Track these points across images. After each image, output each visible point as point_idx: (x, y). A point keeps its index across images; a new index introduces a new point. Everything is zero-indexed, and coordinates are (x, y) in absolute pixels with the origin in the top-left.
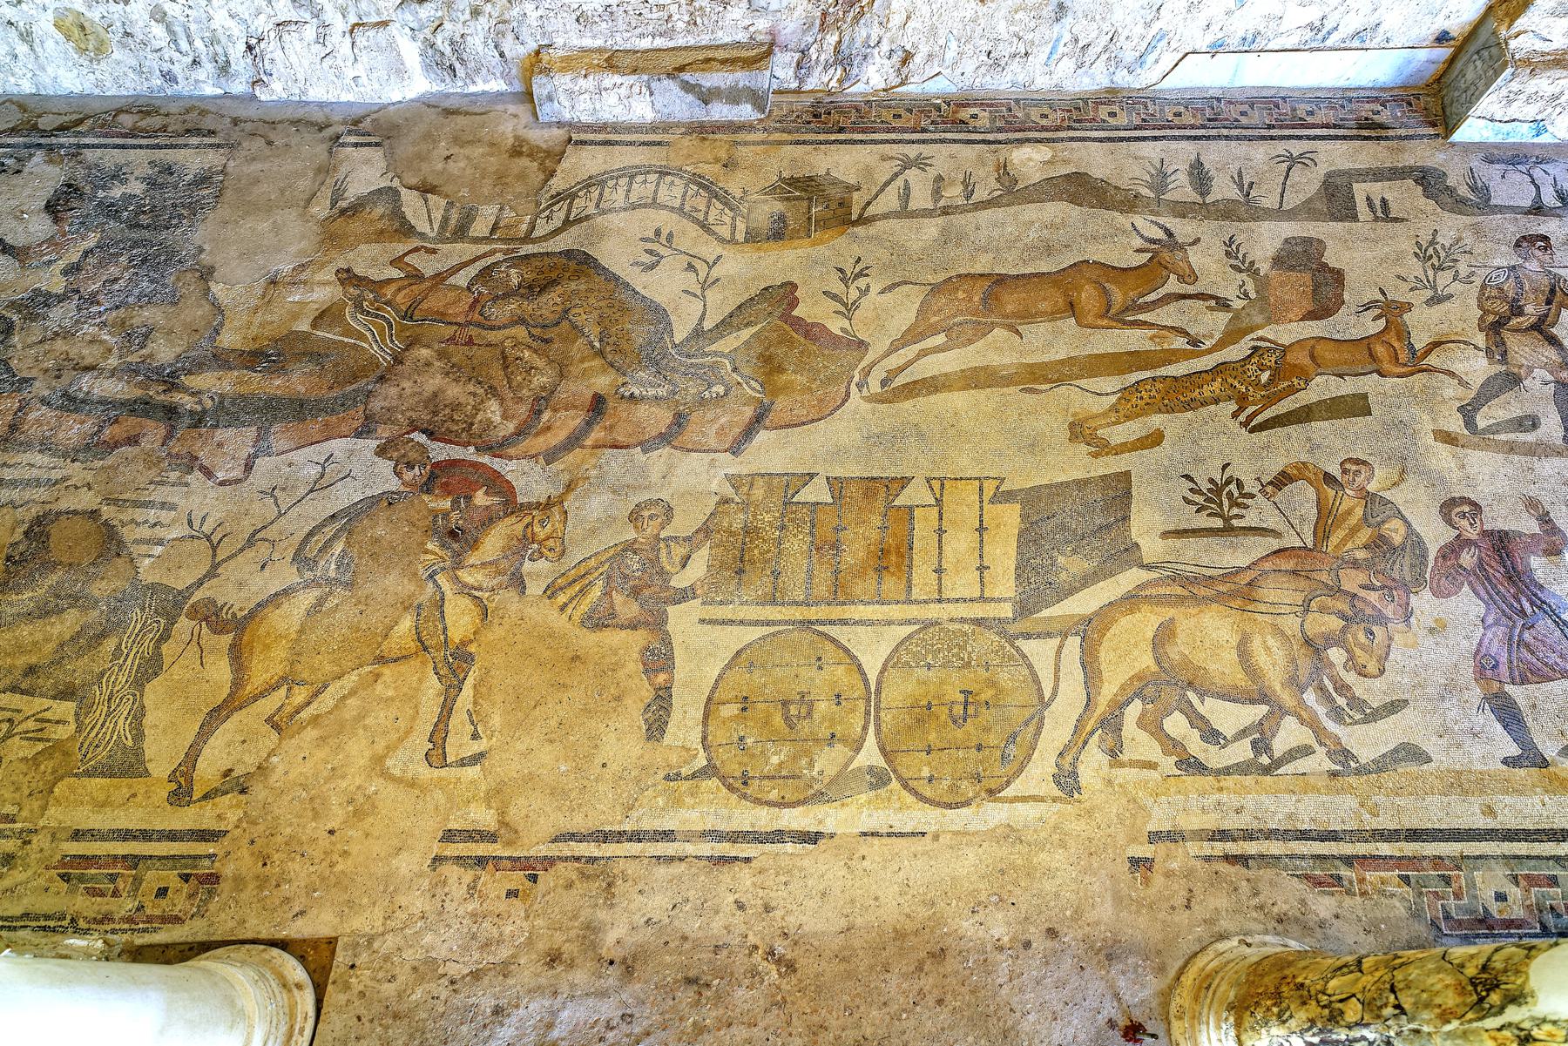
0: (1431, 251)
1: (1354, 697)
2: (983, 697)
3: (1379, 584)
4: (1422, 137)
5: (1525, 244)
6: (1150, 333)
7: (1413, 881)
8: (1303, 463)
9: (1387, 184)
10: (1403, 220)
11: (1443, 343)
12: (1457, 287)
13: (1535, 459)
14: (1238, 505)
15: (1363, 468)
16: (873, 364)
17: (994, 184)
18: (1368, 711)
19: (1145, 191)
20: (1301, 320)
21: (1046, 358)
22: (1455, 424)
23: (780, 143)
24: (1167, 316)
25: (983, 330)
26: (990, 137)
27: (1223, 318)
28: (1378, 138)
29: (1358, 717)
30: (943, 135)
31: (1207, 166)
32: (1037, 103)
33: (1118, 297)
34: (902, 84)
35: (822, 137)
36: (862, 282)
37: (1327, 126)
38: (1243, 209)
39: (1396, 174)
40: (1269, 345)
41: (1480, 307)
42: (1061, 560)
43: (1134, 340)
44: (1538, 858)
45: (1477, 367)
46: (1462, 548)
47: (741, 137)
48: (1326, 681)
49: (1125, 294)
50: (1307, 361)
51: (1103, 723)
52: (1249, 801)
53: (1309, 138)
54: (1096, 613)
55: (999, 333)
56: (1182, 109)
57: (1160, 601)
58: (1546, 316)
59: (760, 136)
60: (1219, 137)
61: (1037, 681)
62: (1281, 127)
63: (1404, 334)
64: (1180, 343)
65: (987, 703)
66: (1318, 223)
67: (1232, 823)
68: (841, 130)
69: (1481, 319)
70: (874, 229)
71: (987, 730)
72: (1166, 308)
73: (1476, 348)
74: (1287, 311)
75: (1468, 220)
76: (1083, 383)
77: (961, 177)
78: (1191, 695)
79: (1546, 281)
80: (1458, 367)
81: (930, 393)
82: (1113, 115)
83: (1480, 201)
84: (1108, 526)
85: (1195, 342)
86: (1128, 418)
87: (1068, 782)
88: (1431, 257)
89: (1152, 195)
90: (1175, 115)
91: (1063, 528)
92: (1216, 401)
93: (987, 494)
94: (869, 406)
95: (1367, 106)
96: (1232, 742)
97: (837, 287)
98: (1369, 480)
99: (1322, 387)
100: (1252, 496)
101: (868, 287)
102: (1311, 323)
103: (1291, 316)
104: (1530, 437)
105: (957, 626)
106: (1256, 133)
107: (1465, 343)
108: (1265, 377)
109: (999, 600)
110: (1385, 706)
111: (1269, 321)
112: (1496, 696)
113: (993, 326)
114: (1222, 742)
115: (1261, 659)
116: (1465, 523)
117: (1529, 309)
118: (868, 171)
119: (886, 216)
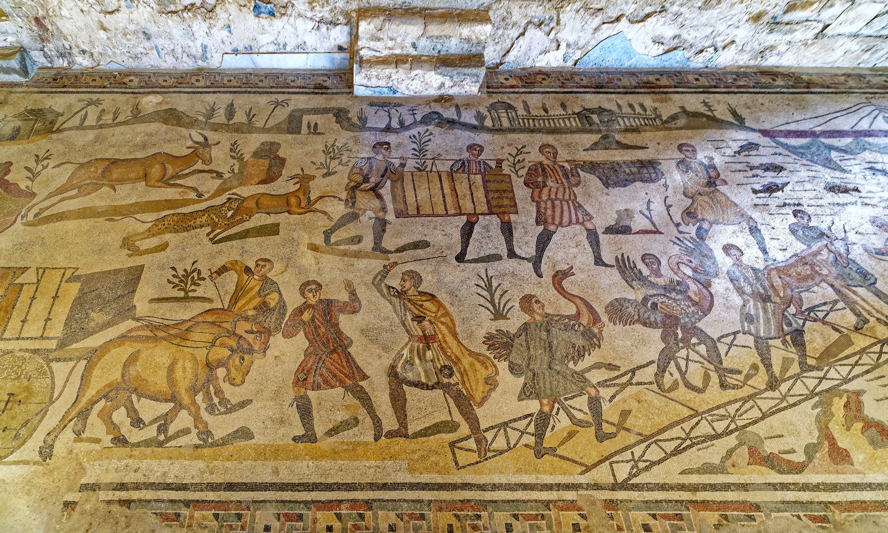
1: (224, 398)
2: (19, 397)
3: (256, 330)
4: (343, 93)
6: (180, 190)
7: (220, 517)
8: (236, 261)
9: (320, 116)
10: (322, 134)
11: (324, 197)
12: (340, 168)
13: (356, 259)
14: (195, 284)
15: (268, 264)
16: (35, 205)
17: (129, 113)
18: (229, 406)
19: (201, 118)
20: (257, 184)
21: (124, 203)
22: (319, 240)
23: (31, 92)
24: (190, 182)
25: (97, 187)
26: (136, 91)
27: (218, 182)
28: (322, 93)
29: (222, 410)
30: (113, 90)
31: (235, 106)
32: (163, 75)
33: (170, 171)
34: (98, 65)
35: (53, 90)
36: (45, 163)
37: (300, 87)
38: (248, 127)
39: (326, 111)
40: (236, 197)
41: (349, 178)
42: (93, 315)
43: (170, 193)
44: (295, 502)
45: (338, 209)
46: (305, 309)
47: (14, 89)
48: (211, 387)
49: (174, 170)
50: (254, 206)
51: (79, 414)
52: (144, 464)
53: (289, 93)
54: (101, 347)
55: (105, 189)
56: (232, 78)
57: (138, 339)
58: (379, 183)
59: (24, 89)
60: (245, 92)
61: (53, 388)
62: (277, 88)
63: (306, 192)
64: (192, 195)
65: (20, 401)
66: (280, 135)
67: (131, 478)
68: (64, 87)
69: (348, 184)
70: (61, 136)
71: (13, 418)
72: (192, 177)
73: (340, 199)
74: (252, 179)
75: (352, 134)
76: (138, 216)
77: (114, 110)
78: (134, 397)
79: (384, 165)
80: (329, 210)
81: (57, 221)
82: (198, 81)
83: (362, 124)
84: (123, 296)
85: (200, 195)
86: (153, 235)
87: (46, 452)
88: (330, 152)
89: (204, 120)
90: (228, 81)
91: (99, 296)
92: (201, 227)
93: (67, 276)
94: (23, 227)
95: (321, 78)
96: (148, 426)
97: (32, 164)
98: (270, 270)
99: (259, 220)
100: (204, 279)
101: (48, 164)
102: (262, 186)
103: (252, 182)
104: (354, 248)
105: (22, 354)
106: (264, 90)
107: (334, 197)
108: (230, 214)
109: (52, 338)
110: (239, 403)
111: (240, 185)
112: (301, 397)
113: (103, 185)
114: (142, 426)
115: (179, 374)
116: (311, 295)
117: (372, 180)
118: (70, 107)
119: (70, 129)
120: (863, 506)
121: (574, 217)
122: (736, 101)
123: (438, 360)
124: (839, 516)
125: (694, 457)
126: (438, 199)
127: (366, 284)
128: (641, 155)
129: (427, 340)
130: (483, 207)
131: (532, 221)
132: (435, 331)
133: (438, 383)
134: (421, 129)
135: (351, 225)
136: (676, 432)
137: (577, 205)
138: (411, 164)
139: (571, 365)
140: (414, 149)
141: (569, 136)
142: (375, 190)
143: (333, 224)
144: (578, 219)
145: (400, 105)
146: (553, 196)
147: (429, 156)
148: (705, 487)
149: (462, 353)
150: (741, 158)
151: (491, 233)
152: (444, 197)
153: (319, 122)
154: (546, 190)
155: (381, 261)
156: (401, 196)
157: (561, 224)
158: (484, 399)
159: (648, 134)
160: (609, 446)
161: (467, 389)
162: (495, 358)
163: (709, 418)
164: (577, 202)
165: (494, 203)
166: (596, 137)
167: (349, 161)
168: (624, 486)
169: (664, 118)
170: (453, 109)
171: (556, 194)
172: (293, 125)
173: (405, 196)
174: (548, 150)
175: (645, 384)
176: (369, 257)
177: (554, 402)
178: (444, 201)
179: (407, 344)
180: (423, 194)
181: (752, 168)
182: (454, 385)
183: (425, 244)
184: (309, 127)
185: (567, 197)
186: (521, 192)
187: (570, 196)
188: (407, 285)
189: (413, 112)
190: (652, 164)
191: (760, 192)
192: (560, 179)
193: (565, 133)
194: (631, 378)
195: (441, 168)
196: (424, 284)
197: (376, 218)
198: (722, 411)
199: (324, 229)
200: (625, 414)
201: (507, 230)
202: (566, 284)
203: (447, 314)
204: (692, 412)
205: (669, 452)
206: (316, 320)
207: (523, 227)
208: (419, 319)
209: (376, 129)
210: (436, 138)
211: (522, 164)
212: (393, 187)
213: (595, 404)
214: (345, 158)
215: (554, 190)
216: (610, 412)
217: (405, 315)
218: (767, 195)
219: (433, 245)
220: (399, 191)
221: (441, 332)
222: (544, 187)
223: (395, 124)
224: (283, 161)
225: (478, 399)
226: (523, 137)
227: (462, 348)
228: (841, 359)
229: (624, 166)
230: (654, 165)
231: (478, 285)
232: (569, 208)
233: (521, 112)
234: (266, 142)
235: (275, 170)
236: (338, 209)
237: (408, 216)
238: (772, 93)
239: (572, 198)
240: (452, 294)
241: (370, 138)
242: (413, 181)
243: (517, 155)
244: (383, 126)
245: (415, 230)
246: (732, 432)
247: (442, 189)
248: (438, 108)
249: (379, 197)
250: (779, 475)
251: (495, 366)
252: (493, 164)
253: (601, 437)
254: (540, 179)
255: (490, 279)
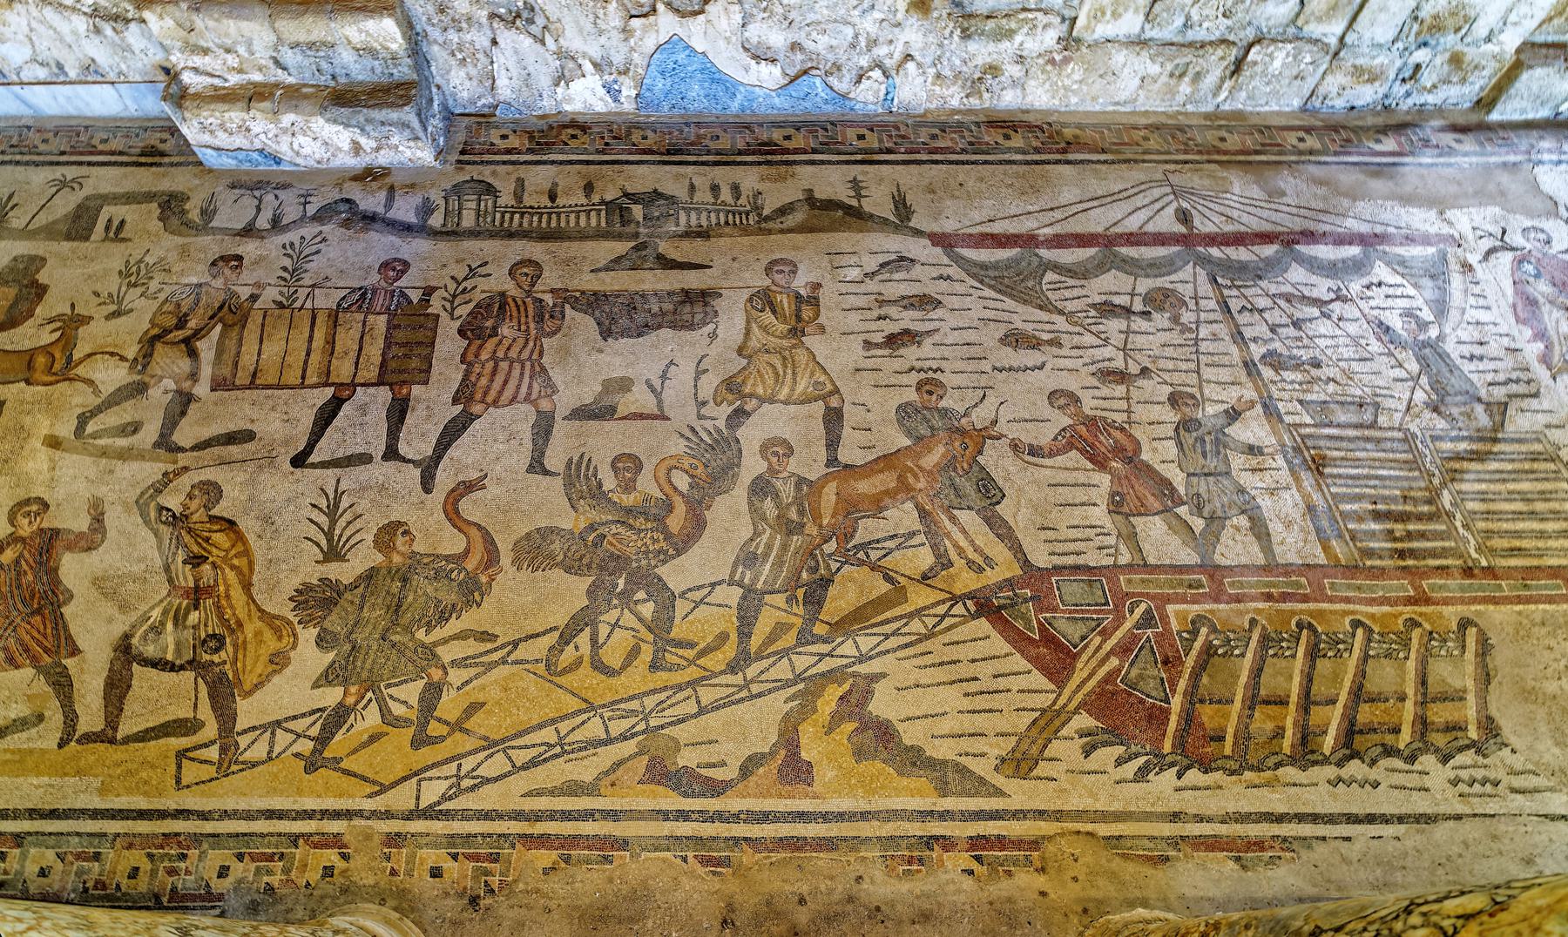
0: (134, 269)
5: (221, 264)
120: (796, 844)
121: (524, 390)
122: (909, 178)
123: (206, 625)
124: (747, 857)
125: (558, 772)
126: (296, 359)
127: (125, 504)
128: (693, 280)
129: (197, 594)
130: (371, 373)
131: (448, 397)
132: (216, 581)
133: (190, 662)
134: (309, 231)
135: (128, 405)
136: (548, 735)
137: (538, 369)
138: (271, 294)
139: (420, 634)
140: (285, 269)
141: (575, 245)
142: (189, 347)
143: (98, 401)
144: (529, 394)
145: (285, 186)
146: (500, 354)
147: (307, 281)
148: (552, 816)
149: (249, 616)
150: (872, 286)
151: (366, 419)
152: (308, 354)
153: (128, 219)
154: (490, 345)
155: (161, 465)
156: (233, 352)
157: (495, 403)
158: (257, 686)
159: (722, 241)
160: (427, 754)
161: (236, 673)
162: (300, 622)
163: (607, 715)
164: (541, 366)
165: (393, 365)
166: (622, 247)
167: (160, 291)
168: (430, 813)
169: (766, 212)
170: (382, 196)
171: (508, 349)
172: (79, 226)
173: (239, 353)
174: (525, 270)
175: (527, 662)
176: (143, 458)
177: (367, 690)
178: (306, 362)
179: (161, 601)
180: (273, 349)
181: (882, 303)
182: (219, 664)
183: (249, 436)
184: (107, 228)
185: (525, 355)
186: (448, 344)
187: (532, 352)
188: (194, 505)
189: (305, 200)
190: (704, 297)
191: (877, 345)
192: (527, 323)
193: (569, 238)
194: (509, 654)
195: (319, 303)
196: (223, 503)
197: (176, 391)
198: (634, 705)
199: (80, 411)
200: (474, 708)
201: (398, 413)
202: (465, 505)
203: (246, 553)
204: (584, 706)
205: (519, 764)
206: (23, 562)
207: (428, 407)
208: (196, 561)
209: (224, 231)
210: (331, 248)
211: (467, 296)
212: (222, 336)
213: (432, 693)
214: (154, 285)
215: (506, 343)
216: (449, 706)
217: (174, 554)
218: (886, 352)
219: (261, 439)
220: (231, 344)
221: (225, 580)
222: (490, 336)
223: (263, 222)
224: (41, 291)
225: (247, 687)
226: (489, 247)
227: (252, 606)
228: (867, 628)
229: (653, 300)
230: (707, 299)
231: (314, 506)
232: (522, 374)
233: (506, 199)
234: (23, 256)
235: (24, 306)
236: (112, 376)
237: (235, 387)
238: (991, 163)
239: (535, 357)
240: (267, 520)
241: (212, 246)
242: (263, 325)
243: (466, 279)
244: (240, 226)
245: (239, 412)
246: (633, 735)
247: (311, 338)
248: (355, 192)
249: (193, 354)
250: (681, 798)
251: (295, 635)
252: (415, 296)
253: (419, 742)
254: (489, 324)
255: (338, 496)
